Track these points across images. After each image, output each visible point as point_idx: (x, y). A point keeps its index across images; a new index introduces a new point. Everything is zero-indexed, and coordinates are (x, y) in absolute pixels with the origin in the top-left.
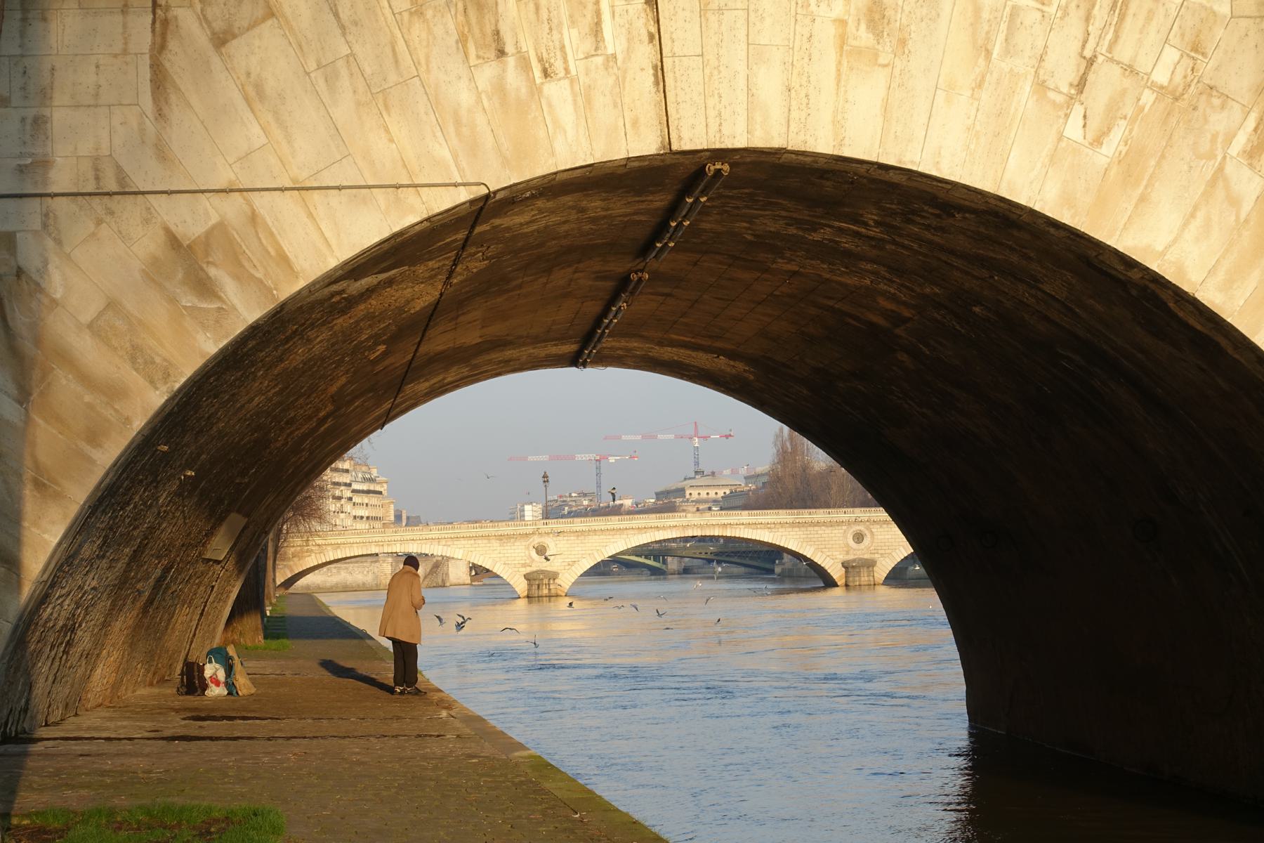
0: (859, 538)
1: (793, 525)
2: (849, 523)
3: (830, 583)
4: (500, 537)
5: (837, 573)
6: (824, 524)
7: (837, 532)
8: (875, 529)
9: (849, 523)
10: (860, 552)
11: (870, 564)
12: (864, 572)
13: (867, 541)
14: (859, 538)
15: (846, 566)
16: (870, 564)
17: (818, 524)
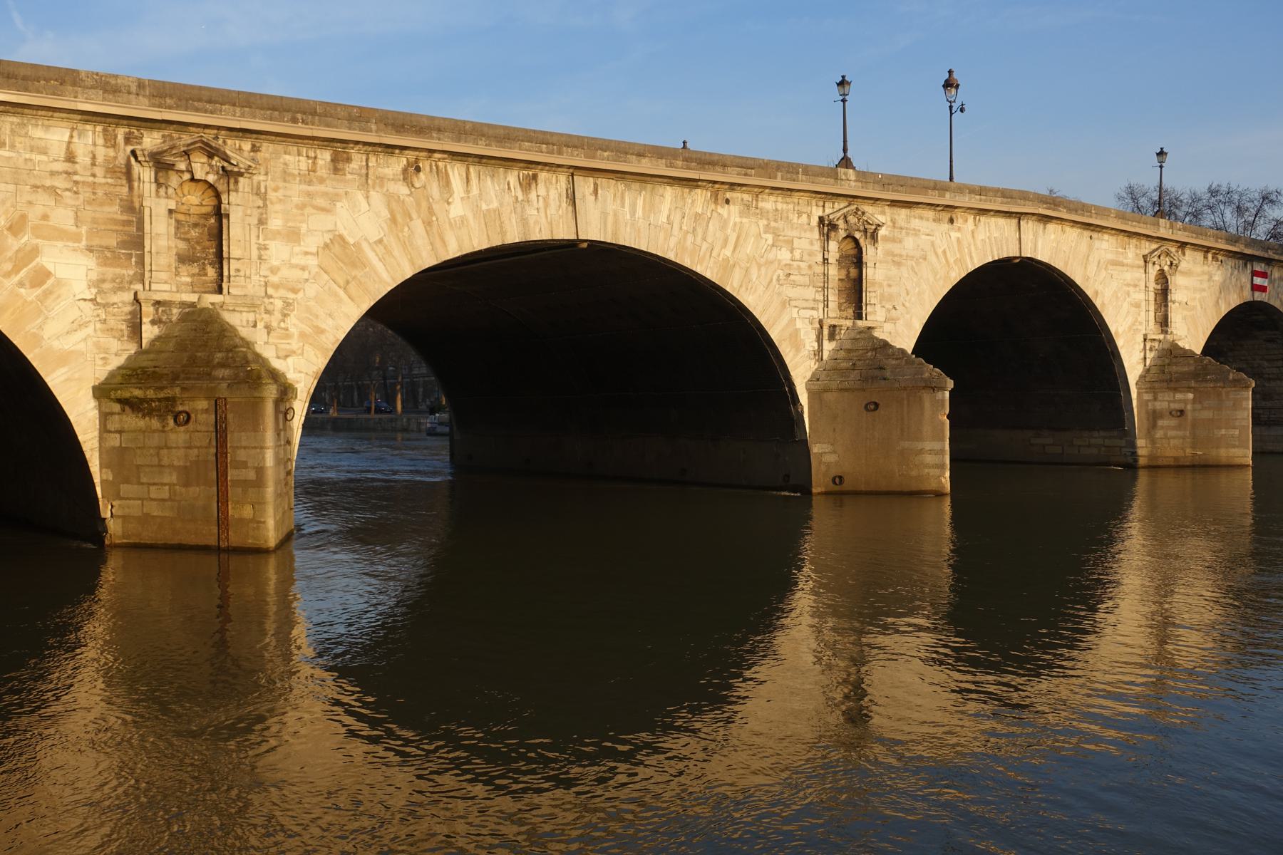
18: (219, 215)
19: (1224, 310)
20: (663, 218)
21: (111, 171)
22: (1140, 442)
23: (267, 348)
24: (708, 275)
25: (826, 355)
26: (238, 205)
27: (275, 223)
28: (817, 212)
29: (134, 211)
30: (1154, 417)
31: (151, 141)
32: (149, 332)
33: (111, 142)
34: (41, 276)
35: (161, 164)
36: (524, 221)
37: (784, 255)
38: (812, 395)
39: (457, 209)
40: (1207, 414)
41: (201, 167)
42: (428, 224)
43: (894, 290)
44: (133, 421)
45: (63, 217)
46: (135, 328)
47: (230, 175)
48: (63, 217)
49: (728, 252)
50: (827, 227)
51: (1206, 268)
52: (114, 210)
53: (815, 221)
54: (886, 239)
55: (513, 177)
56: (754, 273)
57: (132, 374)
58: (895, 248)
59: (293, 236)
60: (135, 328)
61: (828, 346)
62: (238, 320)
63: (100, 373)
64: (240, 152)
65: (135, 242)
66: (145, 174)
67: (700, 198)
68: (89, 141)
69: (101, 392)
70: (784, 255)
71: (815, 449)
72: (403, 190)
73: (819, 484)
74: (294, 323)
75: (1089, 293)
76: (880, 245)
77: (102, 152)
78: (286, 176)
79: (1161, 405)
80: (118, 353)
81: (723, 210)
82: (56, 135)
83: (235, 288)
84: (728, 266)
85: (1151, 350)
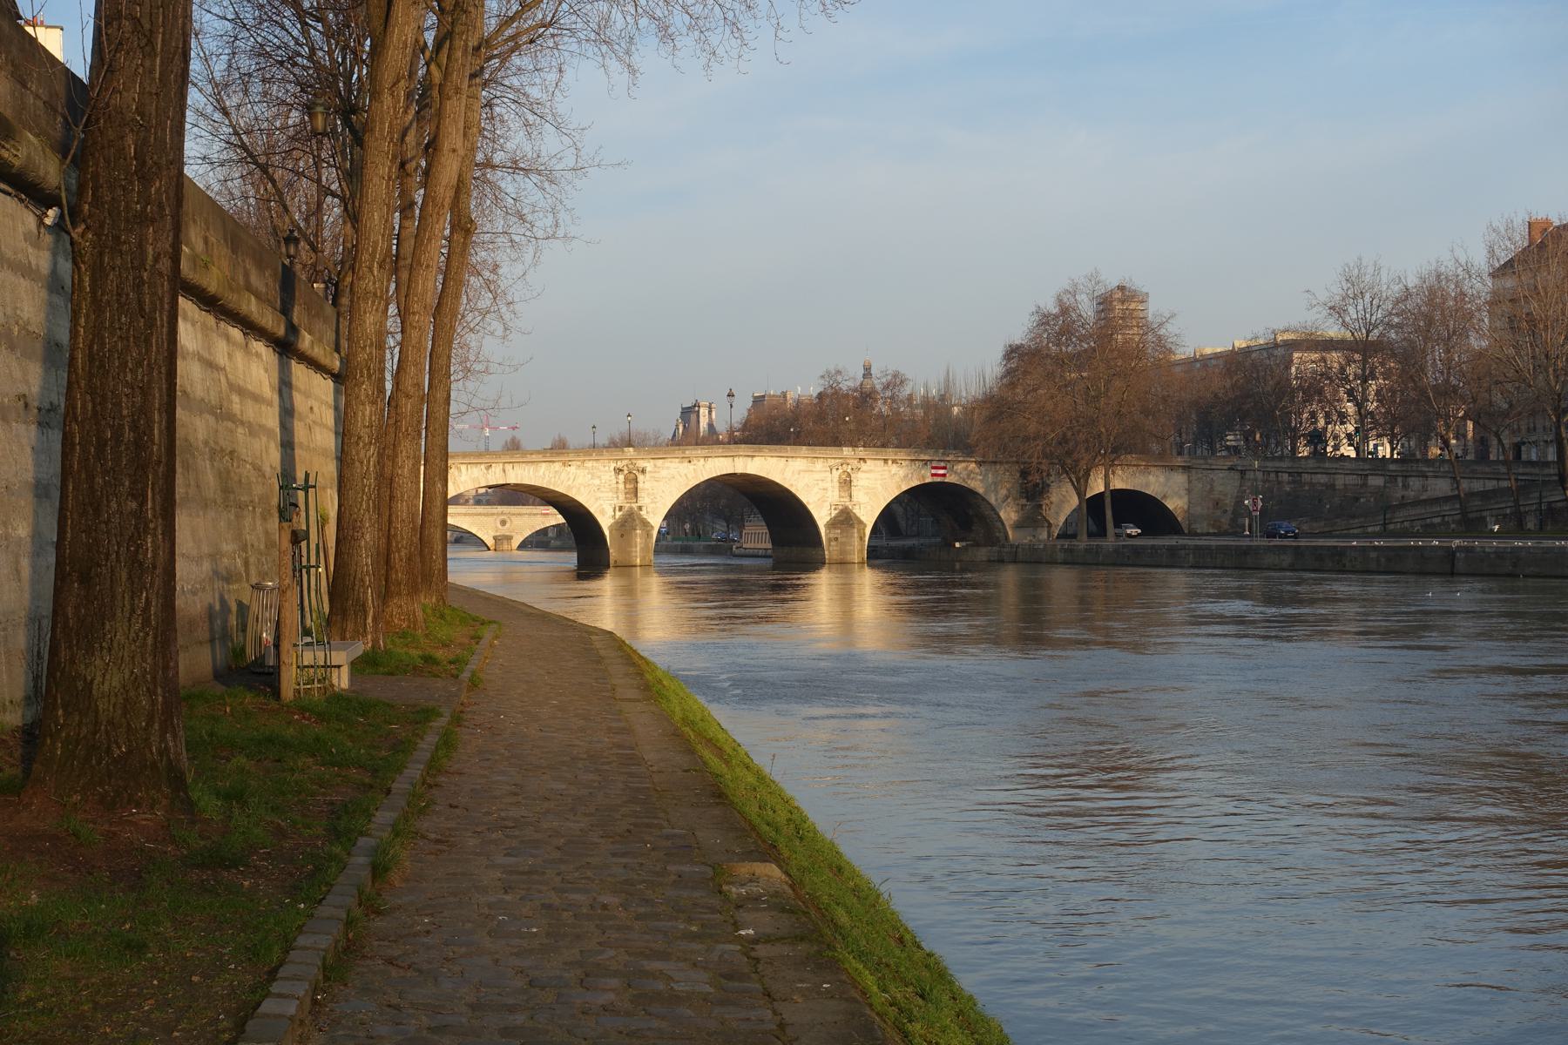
0: (503, 523)
1: (465, 515)
2: (498, 514)
3: (489, 549)
5: (490, 542)
6: (484, 515)
7: (491, 519)
8: (513, 518)
9: (498, 514)
10: (504, 531)
11: (509, 538)
12: (505, 542)
13: (508, 525)
14: (503, 523)
15: (495, 538)
16: (509, 538)
17: (480, 514)
19: (905, 488)
20: (541, 473)
22: (826, 553)
24: (561, 491)
25: (617, 517)
28: (613, 465)
30: (830, 540)
36: (487, 479)
37: (597, 482)
38: (610, 532)
39: (463, 478)
40: (844, 540)
43: (655, 491)
49: (570, 483)
50: (618, 471)
51: (886, 468)
53: (612, 468)
54: (650, 472)
55: (483, 467)
56: (582, 488)
58: (656, 475)
61: (618, 514)
67: (557, 466)
70: (597, 482)
73: (612, 562)
75: (786, 486)
76: (647, 475)
79: (832, 536)
81: (568, 469)
84: (569, 488)
85: (835, 509)
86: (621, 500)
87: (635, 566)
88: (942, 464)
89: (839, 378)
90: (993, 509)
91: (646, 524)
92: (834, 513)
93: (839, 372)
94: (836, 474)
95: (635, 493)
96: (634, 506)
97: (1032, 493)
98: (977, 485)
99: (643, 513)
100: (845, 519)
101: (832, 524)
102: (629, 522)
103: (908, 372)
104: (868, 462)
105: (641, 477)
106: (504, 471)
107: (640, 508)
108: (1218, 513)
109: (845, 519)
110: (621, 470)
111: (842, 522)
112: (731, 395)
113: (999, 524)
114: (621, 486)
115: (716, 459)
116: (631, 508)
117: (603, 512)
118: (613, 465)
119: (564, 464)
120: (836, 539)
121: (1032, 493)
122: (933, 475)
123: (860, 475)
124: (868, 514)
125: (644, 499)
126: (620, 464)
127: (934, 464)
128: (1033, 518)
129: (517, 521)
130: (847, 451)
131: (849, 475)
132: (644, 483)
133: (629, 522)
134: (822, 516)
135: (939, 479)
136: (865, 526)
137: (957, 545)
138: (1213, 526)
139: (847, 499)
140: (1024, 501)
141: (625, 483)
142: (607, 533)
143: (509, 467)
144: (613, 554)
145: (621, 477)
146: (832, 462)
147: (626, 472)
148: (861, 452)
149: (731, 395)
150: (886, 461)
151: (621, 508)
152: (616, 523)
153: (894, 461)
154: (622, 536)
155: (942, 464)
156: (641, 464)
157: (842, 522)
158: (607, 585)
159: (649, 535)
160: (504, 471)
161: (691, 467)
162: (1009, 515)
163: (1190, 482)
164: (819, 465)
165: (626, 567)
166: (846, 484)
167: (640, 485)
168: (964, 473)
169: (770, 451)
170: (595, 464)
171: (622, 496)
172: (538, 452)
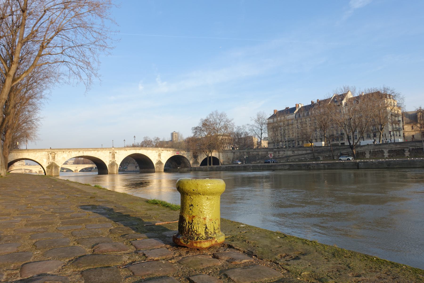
0: (76, 167)
3: (73, 172)
4: (36, 167)
5: (74, 171)
7: (74, 167)
10: (76, 169)
11: (77, 170)
14: (76, 167)
15: (75, 170)
16: (77, 170)
18: (55, 156)
21: (48, 154)
22: (156, 170)
23: (58, 164)
26: (56, 156)
27: (59, 156)
28: (109, 151)
29: (49, 156)
30: (156, 167)
31: (50, 152)
32: (50, 164)
33: (48, 152)
34: (43, 161)
35: (51, 154)
37: (105, 155)
38: (109, 166)
41: (53, 153)
42: (70, 155)
44: (48, 169)
45: (44, 157)
46: (49, 163)
47: (55, 154)
48: (44, 157)
50: (110, 153)
52: (48, 157)
53: (109, 152)
55: (78, 152)
57: (48, 166)
59: (60, 157)
60: (49, 163)
61: (110, 162)
62: (56, 163)
63: (47, 166)
64: (56, 152)
65: (49, 158)
66: (50, 154)
67: (96, 152)
68: (46, 153)
69: (46, 167)
70: (105, 155)
71: (108, 170)
72: (68, 153)
74: (60, 163)
76: (117, 153)
77: (47, 153)
78: (59, 153)
79: (157, 166)
80: (48, 165)
81: (98, 152)
82: (44, 153)
83: (55, 161)
86: (111, 159)
87: (115, 174)
88: (178, 151)
89: (147, 138)
90: (188, 160)
91: (117, 164)
92: (157, 161)
93: (147, 137)
94: (158, 153)
95: (114, 157)
96: (114, 160)
97: (195, 157)
98: (185, 156)
99: (116, 162)
100: (160, 163)
101: (157, 164)
102: (113, 164)
103: (159, 137)
104: (164, 151)
105: (115, 154)
106: (83, 153)
107: (115, 161)
108: (229, 160)
109: (160, 163)
110: (111, 152)
111: (159, 163)
112: (135, 137)
113: (189, 163)
114: (111, 156)
115: (132, 150)
116: (113, 161)
117: (107, 162)
118: (109, 151)
119: (98, 151)
120: (158, 167)
121: (195, 157)
122: (177, 154)
123: (162, 153)
124: (164, 161)
125: (116, 159)
126: (111, 151)
127: (177, 151)
128: (196, 162)
129: (79, 167)
130: (160, 149)
131: (160, 154)
132: (116, 155)
133: (113, 164)
134: (155, 162)
135: (177, 154)
136: (163, 164)
137: (179, 168)
138: (228, 163)
139: (160, 159)
140: (194, 159)
141: (112, 155)
142: (107, 166)
143: (84, 152)
144: (109, 171)
145: (111, 154)
146: (156, 151)
147: (112, 153)
148: (162, 149)
149: (135, 137)
150: (167, 151)
151: (111, 161)
152: (110, 164)
153: (169, 151)
154: (111, 167)
155: (178, 151)
156: (115, 151)
157: (159, 163)
158: (107, 178)
159: (117, 167)
160: (83, 153)
161: (127, 152)
162: (191, 162)
163: (223, 155)
164: (154, 151)
165: (113, 174)
166: (160, 155)
167: (115, 156)
168: (183, 153)
169: (144, 148)
170: (105, 151)
171: (111, 158)
172: (92, 148)
